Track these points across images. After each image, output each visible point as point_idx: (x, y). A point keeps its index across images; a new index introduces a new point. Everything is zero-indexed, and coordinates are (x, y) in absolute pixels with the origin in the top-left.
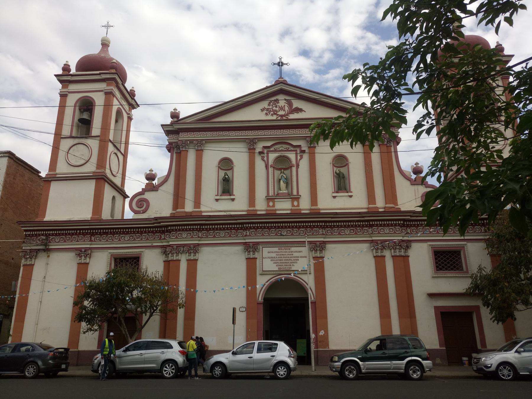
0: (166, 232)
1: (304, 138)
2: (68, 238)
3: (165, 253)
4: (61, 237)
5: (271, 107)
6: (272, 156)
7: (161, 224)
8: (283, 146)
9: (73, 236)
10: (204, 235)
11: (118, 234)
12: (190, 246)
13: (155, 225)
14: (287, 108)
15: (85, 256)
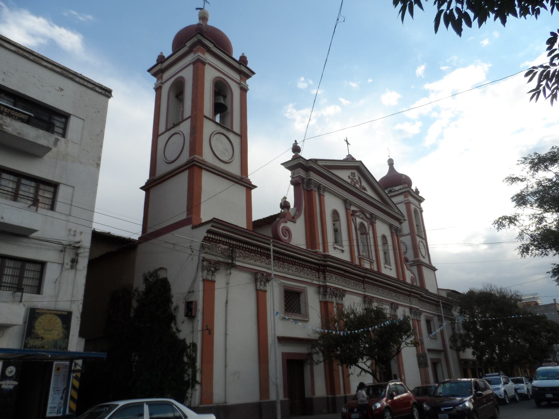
0: (321, 272)
1: (371, 214)
2: (247, 255)
3: (325, 294)
4: (240, 251)
5: (352, 177)
6: (359, 220)
7: (329, 263)
8: (362, 215)
9: (252, 254)
10: (344, 281)
11: (287, 262)
12: (340, 291)
13: (321, 262)
14: (359, 184)
15: (265, 282)
